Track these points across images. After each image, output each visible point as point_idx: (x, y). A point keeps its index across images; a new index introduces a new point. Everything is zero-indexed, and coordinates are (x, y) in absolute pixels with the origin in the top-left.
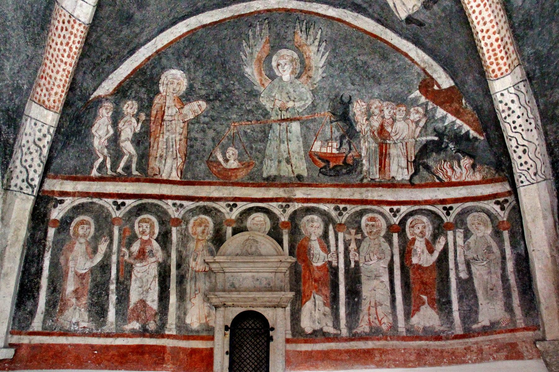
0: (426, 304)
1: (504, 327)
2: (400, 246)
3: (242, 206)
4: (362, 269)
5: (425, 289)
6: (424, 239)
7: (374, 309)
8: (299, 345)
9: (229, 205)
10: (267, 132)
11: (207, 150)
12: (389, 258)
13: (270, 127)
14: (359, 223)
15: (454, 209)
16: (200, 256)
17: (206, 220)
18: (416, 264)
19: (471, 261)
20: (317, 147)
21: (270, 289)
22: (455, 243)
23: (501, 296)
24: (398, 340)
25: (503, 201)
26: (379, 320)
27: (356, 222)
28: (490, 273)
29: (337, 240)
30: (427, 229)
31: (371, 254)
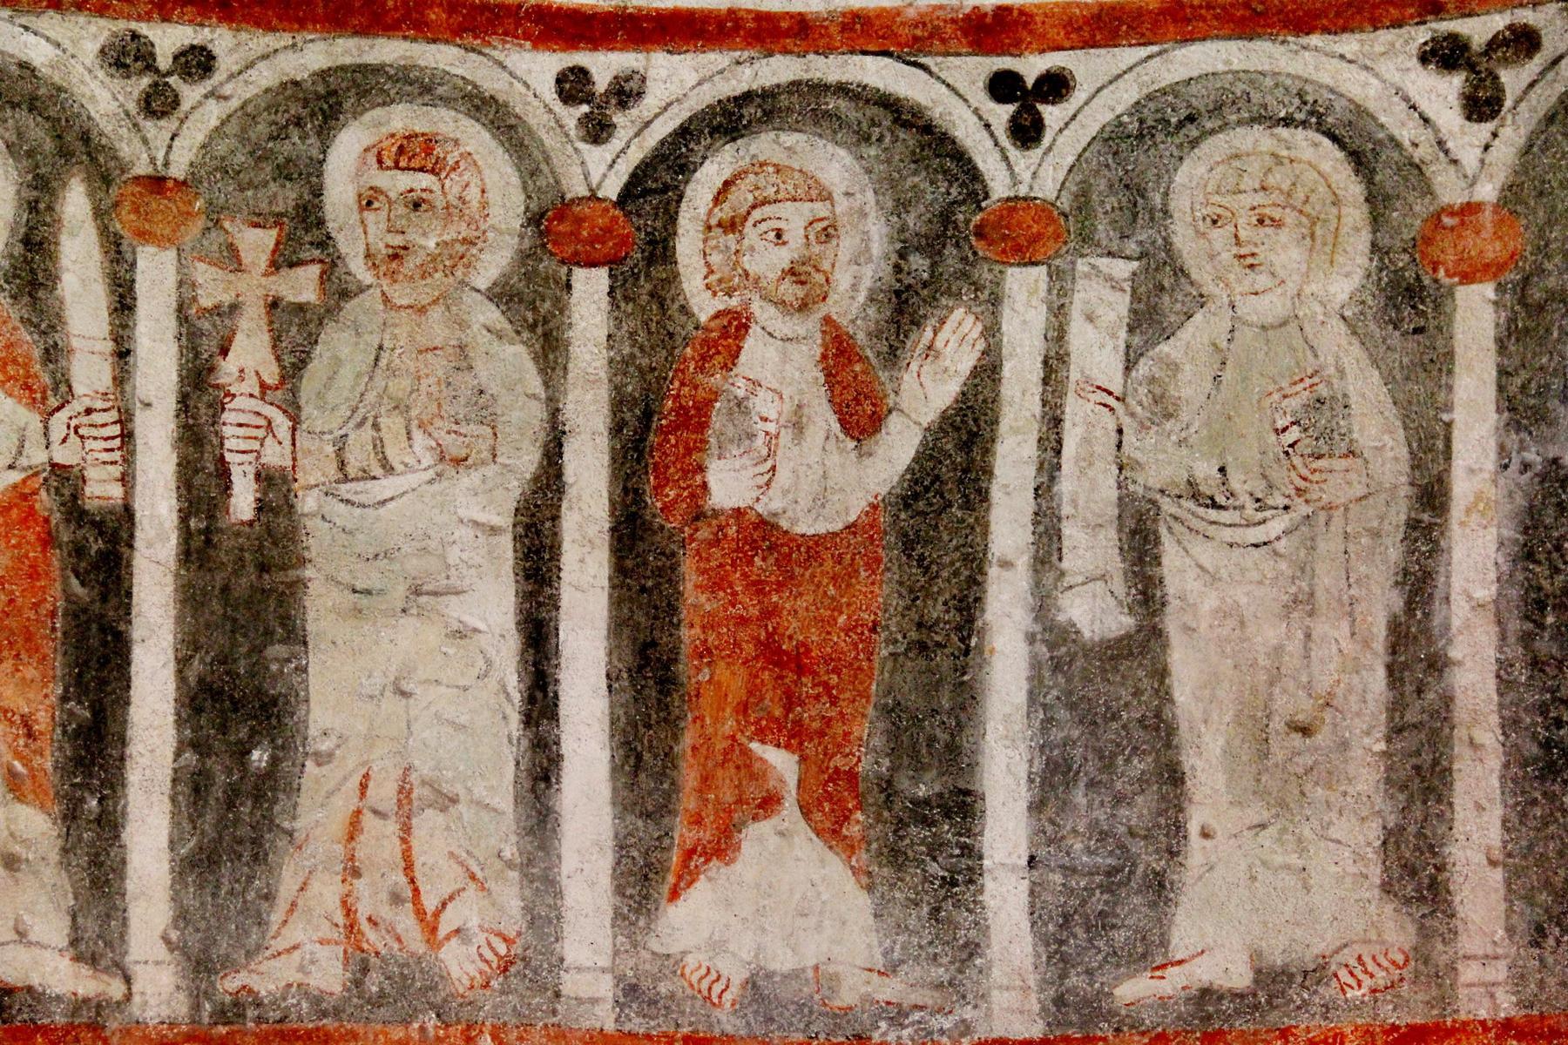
0: (790, 807)
1: (1358, 1007)
2: (620, 367)
4: (318, 540)
5: (791, 700)
6: (807, 326)
7: (392, 827)
12: (529, 460)
14: (310, 176)
15: (1078, 97)
18: (738, 513)
19: (1167, 505)
22: (1054, 367)
23: (1366, 778)
25: (1494, 44)
26: (420, 913)
27: (285, 172)
28: (1303, 603)
29: (123, 303)
30: (846, 244)
31: (392, 425)
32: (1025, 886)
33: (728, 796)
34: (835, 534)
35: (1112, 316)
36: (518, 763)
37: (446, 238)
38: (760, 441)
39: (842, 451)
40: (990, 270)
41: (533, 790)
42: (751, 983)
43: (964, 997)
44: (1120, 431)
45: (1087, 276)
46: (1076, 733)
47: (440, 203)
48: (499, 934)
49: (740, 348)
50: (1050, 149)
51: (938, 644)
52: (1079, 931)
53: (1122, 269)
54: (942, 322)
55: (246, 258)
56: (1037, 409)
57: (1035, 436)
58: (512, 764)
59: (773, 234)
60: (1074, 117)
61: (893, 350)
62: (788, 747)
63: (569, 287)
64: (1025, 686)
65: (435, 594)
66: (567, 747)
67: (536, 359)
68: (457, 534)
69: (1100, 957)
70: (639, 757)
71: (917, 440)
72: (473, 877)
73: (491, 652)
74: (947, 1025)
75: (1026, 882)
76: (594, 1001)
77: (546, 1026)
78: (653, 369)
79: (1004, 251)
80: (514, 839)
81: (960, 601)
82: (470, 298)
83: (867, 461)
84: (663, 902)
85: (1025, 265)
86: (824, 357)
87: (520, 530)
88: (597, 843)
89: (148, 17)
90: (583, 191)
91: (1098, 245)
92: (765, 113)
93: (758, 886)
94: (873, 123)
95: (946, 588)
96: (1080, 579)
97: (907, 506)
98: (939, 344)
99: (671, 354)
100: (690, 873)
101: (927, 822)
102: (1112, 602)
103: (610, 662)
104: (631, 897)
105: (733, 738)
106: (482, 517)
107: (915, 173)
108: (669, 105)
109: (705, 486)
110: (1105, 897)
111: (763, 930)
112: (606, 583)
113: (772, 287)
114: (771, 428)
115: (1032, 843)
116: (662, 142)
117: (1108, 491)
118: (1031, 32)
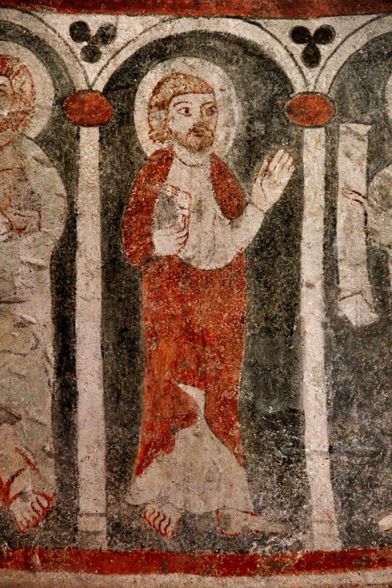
0: (201, 419)
2: (105, 180)
5: (199, 360)
6: (203, 159)
15: (338, 40)
18: (169, 258)
24: (74, 568)
30: (222, 117)
32: (327, 463)
33: (168, 414)
34: (220, 270)
35: (359, 154)
36: (53, 397)
37: (13, 110)
38: (180, 220)
39: (223, 225)
40: (296, 130)
41: (62, 412)
42: (182, 521)
43: (298, 527)
44: (366, 214)
45: (345, 133)
46: (351, 377)
47: (9, 92)
48: (44, 495)
49: (168, 170)
50: (323, 67)
51: (276, 329)
52: (358, 488)
53: (363, 129)
54: (272, 157)
56: (323, 203)
57: (322, 217)
58: (50, 398)
59: (184, 110)
60: (335, 51)
61: (247, 171)
62: (199, 386)
63: (78, 137)
64: (323, 351)
65: (8, 303)
66: (81, 386)
67: (61, 175)
68: (20, 270)
69: (370, 503)
70: (119, 393)
71: (261, 219)
72: (29, 462)
73: (39, 334)
74: (289, 544)
75: (328, 461)
76: (96, 533)
77: (69, 548)
78: (123, 181)
79: (302, 120)
80: (51, 439)
81: (287, 306)
82: (26, 143)
83: (236, 230)
84: (134, 475)
85: (314, 127)
86: (212, 175)
87: (54, 267)
88: (97, 442)
90: (84, 87)
91: (350, 117)
92: (178, 47)
93: (184, 464)
94: (234, 53)
95: (280, 298)
96: (349, 293)
97: (257, 254)
98: (271, 168)
99: (133, 173)
100: (148, 458)
101: (275, 428)
102: (366, 306)
103: (102, 340)
104: (116, 472)
105: (169, 381)
106: (34, 261)
107: (256, 79)
108: (129, 42)
109: (151, 243)
110: (371, 469)
111: (188, 490)
112: (100, 296)
113: (184, 138)
114: (186, 212)
115: (330, 439)
116: (126, 62)
117: (361, 246)
118: (312, 7)
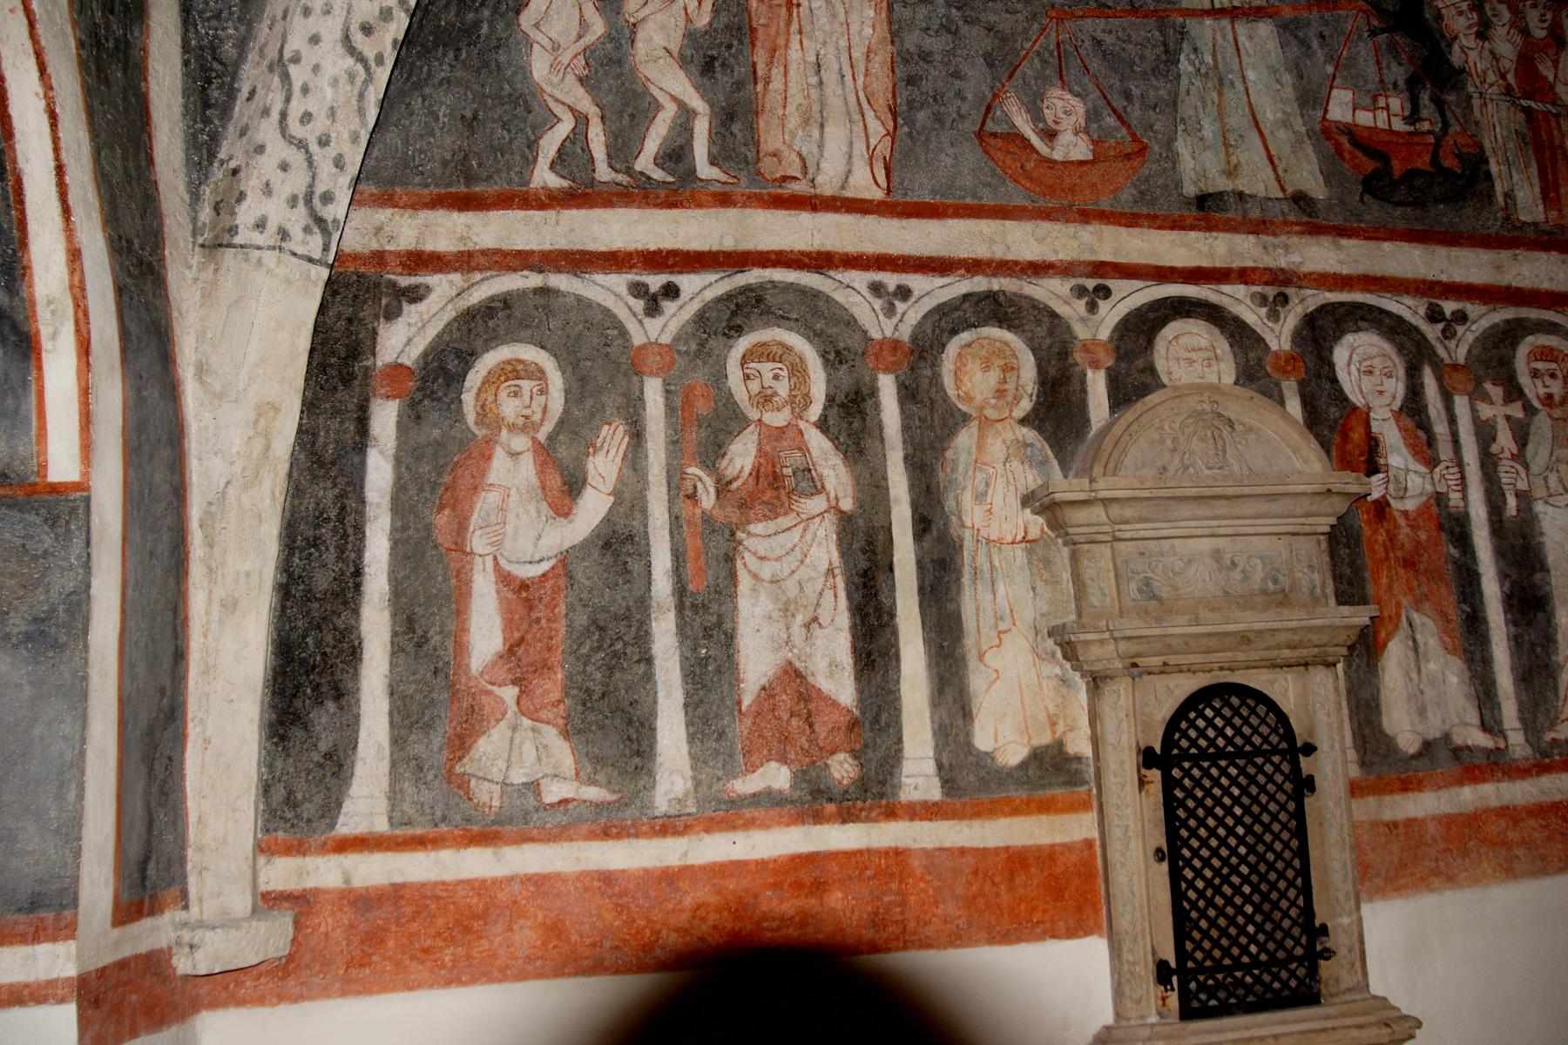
3: (1130, 296)
8: (1387, 799)
9: (1080, 291)
10: (1172, 46)
11: (970, 96)
13: (1183, 34)
16: (1000, 482)
17: (1006, 344)
20: (1340, 107)
21: (1280, 597)
29: (1452, 420)
55: (1494, 398)
89: (1439, 298)
